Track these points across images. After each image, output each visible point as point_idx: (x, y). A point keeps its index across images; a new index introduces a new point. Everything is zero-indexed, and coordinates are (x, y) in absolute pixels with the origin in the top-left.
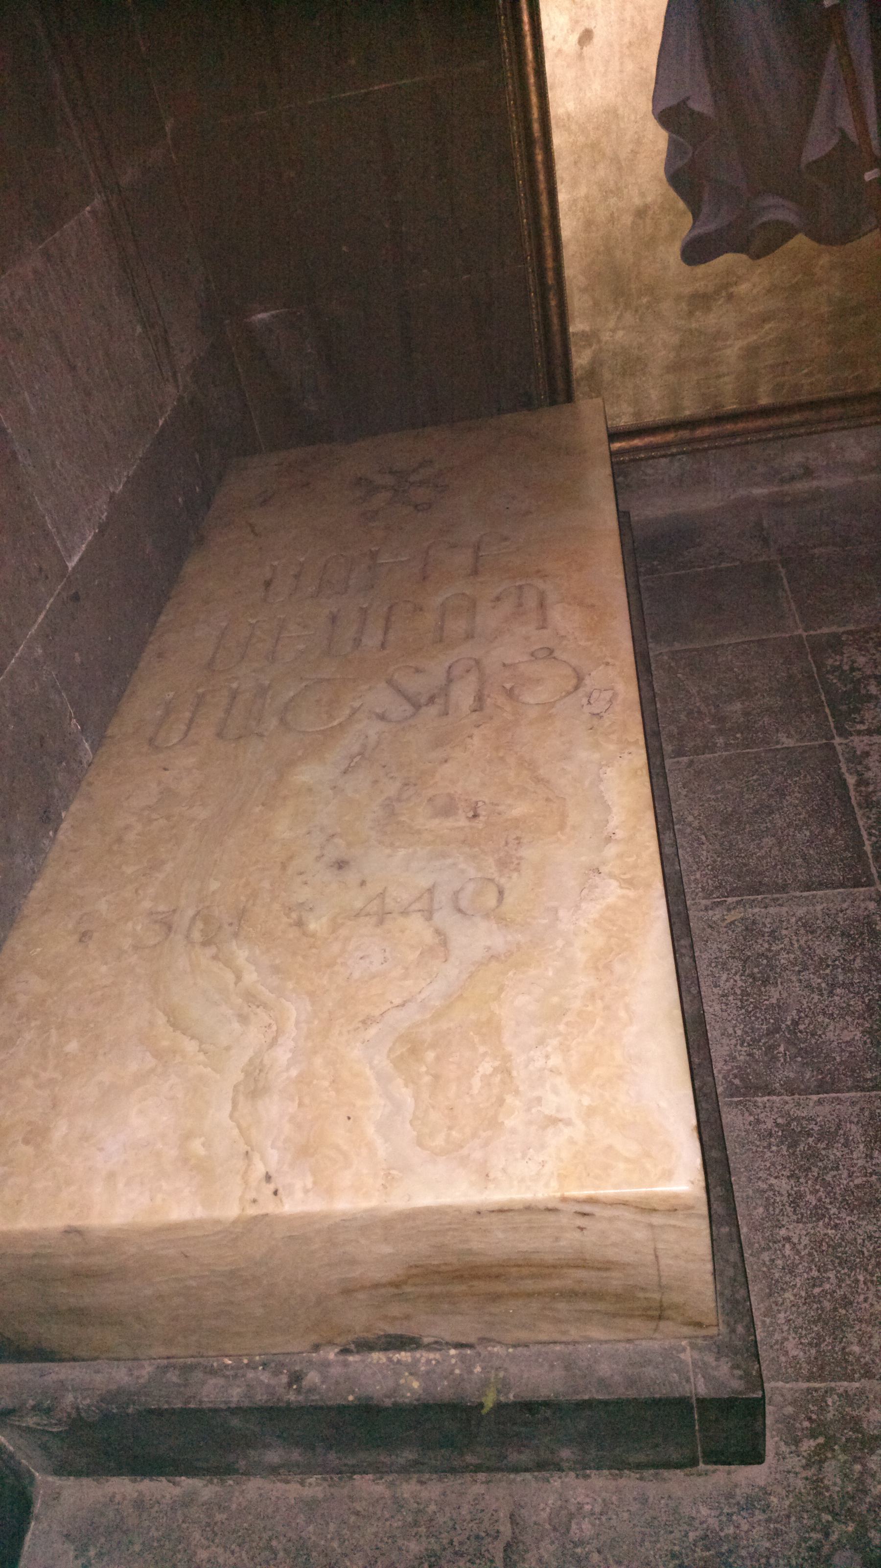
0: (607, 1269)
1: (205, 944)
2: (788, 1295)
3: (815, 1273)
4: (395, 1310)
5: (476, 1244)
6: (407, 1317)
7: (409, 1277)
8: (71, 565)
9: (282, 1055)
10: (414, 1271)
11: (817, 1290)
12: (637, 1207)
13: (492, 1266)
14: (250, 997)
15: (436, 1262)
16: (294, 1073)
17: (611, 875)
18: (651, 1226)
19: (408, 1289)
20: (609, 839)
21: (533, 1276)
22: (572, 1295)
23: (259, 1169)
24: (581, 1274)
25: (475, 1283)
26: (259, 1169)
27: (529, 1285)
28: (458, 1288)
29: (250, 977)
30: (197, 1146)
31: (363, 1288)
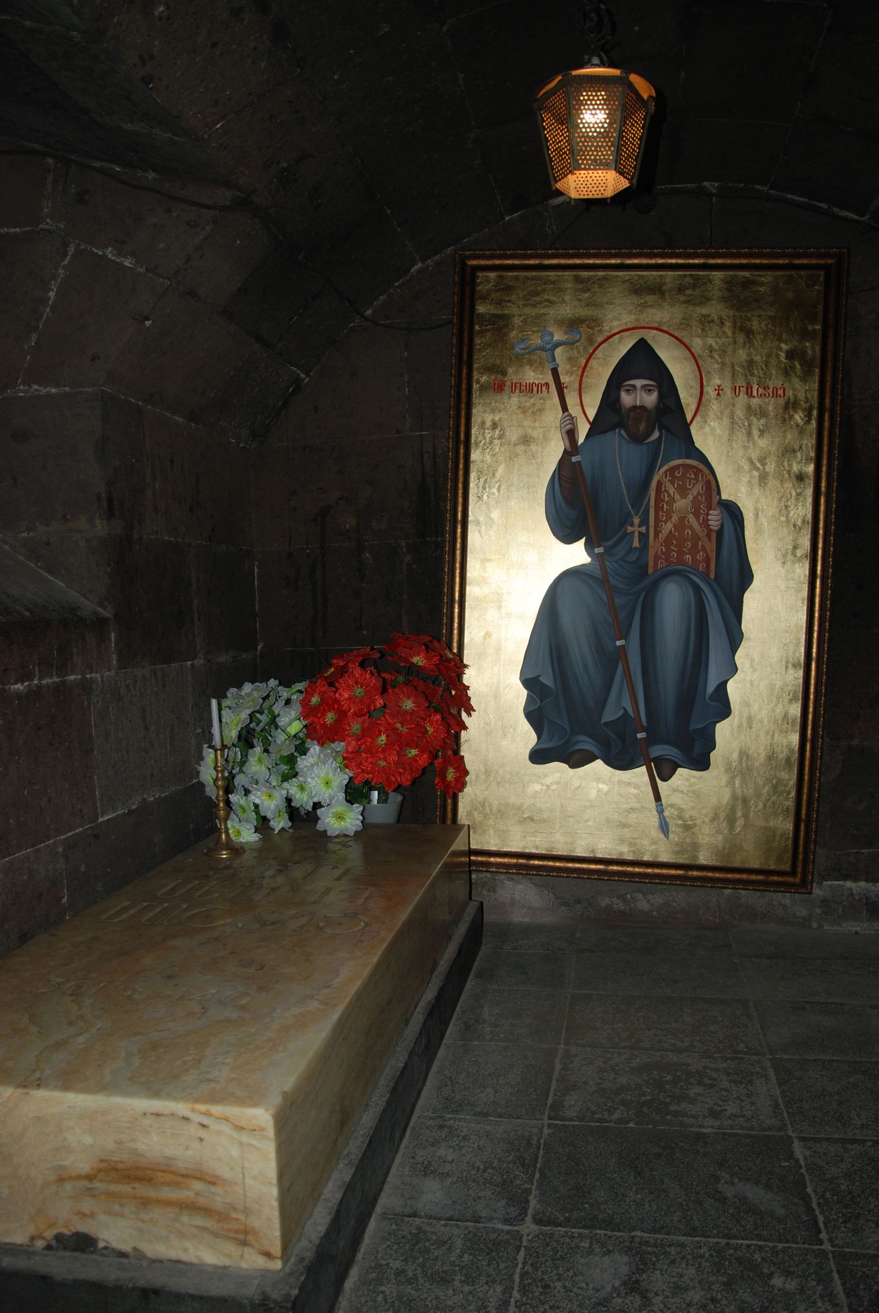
4: (87, 1206)
5: (140, 1146)
6: (92, 1215)
7: (100, 1170)
8: (100, 820)
10: (103, 1165)
12: (233, 1124)
13: (146, 1169)
15: (115, 1159)
16: (82, 1046)
18: (241, 1144)
19: (97, 1184)
21: (170, 1184)
22: (191, 1207)
23: (37, 1075)
24: (198, 1186)
25: (137, 1185)
26: (37, 1075)
28: (126, 1188)
31: (70, 1178)
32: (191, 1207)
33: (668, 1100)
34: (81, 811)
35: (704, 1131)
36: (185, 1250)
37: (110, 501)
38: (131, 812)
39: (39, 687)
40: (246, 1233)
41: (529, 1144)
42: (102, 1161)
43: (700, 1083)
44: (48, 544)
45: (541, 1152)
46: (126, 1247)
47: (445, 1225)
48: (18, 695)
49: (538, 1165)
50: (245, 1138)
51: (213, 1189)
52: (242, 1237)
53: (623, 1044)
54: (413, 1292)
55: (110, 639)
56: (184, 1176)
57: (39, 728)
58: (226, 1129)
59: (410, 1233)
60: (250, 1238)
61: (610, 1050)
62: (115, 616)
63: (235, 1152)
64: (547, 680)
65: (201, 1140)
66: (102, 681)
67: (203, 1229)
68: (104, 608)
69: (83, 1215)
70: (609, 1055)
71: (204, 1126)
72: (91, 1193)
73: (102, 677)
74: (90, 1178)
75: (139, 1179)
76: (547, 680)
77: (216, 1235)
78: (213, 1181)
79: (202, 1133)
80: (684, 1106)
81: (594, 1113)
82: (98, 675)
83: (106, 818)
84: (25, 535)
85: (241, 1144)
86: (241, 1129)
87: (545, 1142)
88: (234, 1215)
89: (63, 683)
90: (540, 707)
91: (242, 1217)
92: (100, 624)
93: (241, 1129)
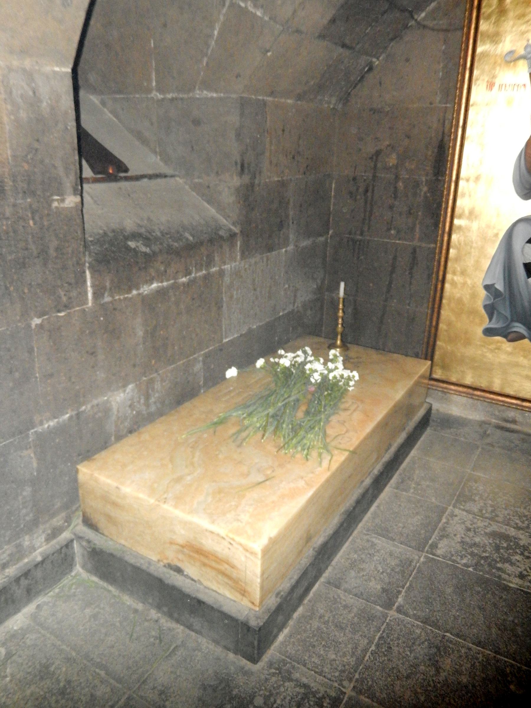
0: (233, 568)
1: (192, 447)
2: (299, 637)
3: (311, 635)
4: (181, 556)
5: (204, 542)
6: (182, 561)
7: (186, 545)
8: (225, 341)
9: (189, 478)
11: (308, 640)
14: (192, 464)
16: (188, 483)
17: (305, 480)
19: (185, 550)
20: (312, 473)
21: (215, 561)
22: (224, 574)
23: (165, 496)
24: (226, 566)
26: (165, 496)
27: (214, 564)
28: (196, 556)
29: (196, 459)
30: (156, 485)
32: (224, 574)
33: (498, 560)
34: (214, 338)
35: (511, 585)
36: (219, 588)
37: (242, 166)
38: (241, 335)
39: (195, 278)
40: (245, 591)
41: (410, 565)
42: (188, 542)
43: (522, 554)
44: (208, 187)
45: (415, 571)
46: (196, 579)
47: (351, 598)
48: (184, 284)
49: (411, 579)
50: (248, 555)
51: (232, 570)
52: (243, 592)
53: (487, 515)
54: (324, 629)
55: (237, 245)
56: (220, 560)
57: (193, 299)
58: (241, 549)
59: (333, 597)
60: (246, 594)
61: (478, 517)
62: (241, 232)
63: (243, 559)
64: (500, 287)
65: (229, 549)
66: (231, 269)
67: (228, 584)
68: (236, 227)
69: (179, 560)
70: (475, 520)
71: (231, 544)
72: (182, 552)
73: (231, 266)
74: (183, 546)
75: (201, 554)
76: (500, 287)
77: (232, 588)
78: (233, 567)
79: (230, 546)
80: (507, 566)
81: (452, 555)
82: (229, 266)
83: (227, 340)
84: (196, 180)
85: (246, 556)
86: (247, 550)
87: (419, 566)
88: (240, 583)
89: (209, 274)
90: (493, 304)
91: (243, 585)
92: (233, 236)
93: (247, 550)
